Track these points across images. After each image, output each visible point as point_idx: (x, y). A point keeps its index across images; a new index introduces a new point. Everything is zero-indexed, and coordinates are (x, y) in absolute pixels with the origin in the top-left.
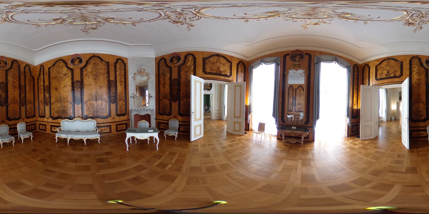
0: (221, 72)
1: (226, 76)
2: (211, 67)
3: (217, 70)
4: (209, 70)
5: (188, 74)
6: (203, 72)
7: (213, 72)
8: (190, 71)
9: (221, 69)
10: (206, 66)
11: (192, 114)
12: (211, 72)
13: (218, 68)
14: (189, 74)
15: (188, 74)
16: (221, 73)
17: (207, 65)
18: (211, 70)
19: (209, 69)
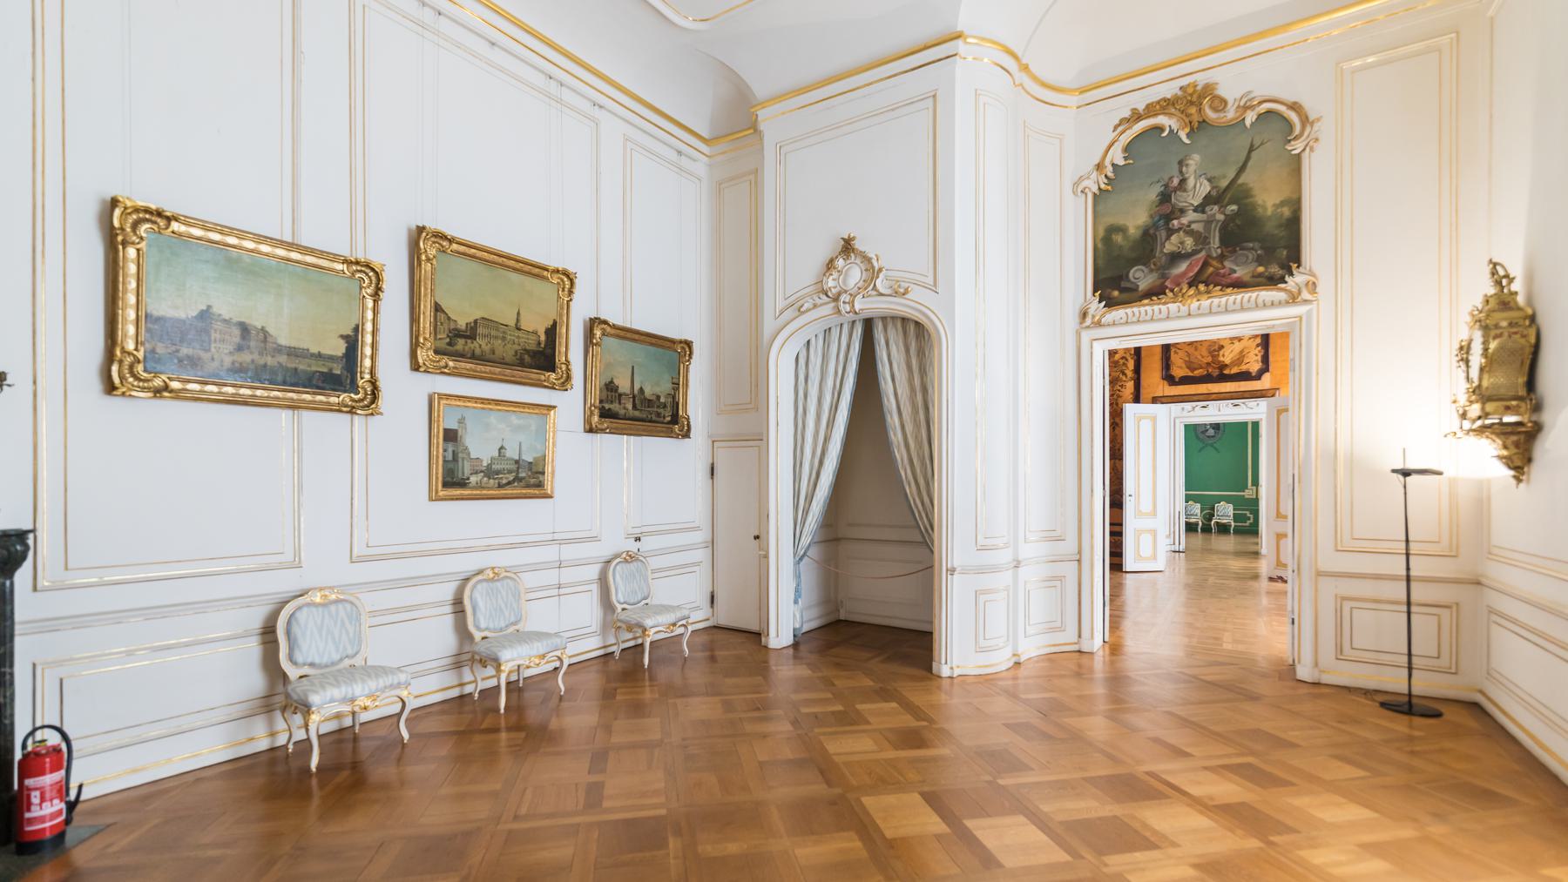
0: (1226, 365)
1: (1245, 376)
2: (1189, 355)
3: (1208, 364)
4: (1181, 367)
5: (1119, 391)
6: (1163, 379)
7: (1196, 372)
8: (1124, 378)
9: (1223, 356)
10: (1172, 353)
11: (1128, 498)
12: (1191, 374)
13: (1213, 356)
14: (1123, 390)
15: (1119, 391)
16: (1225, 372)
17: (1176, 352)
18: (1189, 368)
19: (1184, 366)
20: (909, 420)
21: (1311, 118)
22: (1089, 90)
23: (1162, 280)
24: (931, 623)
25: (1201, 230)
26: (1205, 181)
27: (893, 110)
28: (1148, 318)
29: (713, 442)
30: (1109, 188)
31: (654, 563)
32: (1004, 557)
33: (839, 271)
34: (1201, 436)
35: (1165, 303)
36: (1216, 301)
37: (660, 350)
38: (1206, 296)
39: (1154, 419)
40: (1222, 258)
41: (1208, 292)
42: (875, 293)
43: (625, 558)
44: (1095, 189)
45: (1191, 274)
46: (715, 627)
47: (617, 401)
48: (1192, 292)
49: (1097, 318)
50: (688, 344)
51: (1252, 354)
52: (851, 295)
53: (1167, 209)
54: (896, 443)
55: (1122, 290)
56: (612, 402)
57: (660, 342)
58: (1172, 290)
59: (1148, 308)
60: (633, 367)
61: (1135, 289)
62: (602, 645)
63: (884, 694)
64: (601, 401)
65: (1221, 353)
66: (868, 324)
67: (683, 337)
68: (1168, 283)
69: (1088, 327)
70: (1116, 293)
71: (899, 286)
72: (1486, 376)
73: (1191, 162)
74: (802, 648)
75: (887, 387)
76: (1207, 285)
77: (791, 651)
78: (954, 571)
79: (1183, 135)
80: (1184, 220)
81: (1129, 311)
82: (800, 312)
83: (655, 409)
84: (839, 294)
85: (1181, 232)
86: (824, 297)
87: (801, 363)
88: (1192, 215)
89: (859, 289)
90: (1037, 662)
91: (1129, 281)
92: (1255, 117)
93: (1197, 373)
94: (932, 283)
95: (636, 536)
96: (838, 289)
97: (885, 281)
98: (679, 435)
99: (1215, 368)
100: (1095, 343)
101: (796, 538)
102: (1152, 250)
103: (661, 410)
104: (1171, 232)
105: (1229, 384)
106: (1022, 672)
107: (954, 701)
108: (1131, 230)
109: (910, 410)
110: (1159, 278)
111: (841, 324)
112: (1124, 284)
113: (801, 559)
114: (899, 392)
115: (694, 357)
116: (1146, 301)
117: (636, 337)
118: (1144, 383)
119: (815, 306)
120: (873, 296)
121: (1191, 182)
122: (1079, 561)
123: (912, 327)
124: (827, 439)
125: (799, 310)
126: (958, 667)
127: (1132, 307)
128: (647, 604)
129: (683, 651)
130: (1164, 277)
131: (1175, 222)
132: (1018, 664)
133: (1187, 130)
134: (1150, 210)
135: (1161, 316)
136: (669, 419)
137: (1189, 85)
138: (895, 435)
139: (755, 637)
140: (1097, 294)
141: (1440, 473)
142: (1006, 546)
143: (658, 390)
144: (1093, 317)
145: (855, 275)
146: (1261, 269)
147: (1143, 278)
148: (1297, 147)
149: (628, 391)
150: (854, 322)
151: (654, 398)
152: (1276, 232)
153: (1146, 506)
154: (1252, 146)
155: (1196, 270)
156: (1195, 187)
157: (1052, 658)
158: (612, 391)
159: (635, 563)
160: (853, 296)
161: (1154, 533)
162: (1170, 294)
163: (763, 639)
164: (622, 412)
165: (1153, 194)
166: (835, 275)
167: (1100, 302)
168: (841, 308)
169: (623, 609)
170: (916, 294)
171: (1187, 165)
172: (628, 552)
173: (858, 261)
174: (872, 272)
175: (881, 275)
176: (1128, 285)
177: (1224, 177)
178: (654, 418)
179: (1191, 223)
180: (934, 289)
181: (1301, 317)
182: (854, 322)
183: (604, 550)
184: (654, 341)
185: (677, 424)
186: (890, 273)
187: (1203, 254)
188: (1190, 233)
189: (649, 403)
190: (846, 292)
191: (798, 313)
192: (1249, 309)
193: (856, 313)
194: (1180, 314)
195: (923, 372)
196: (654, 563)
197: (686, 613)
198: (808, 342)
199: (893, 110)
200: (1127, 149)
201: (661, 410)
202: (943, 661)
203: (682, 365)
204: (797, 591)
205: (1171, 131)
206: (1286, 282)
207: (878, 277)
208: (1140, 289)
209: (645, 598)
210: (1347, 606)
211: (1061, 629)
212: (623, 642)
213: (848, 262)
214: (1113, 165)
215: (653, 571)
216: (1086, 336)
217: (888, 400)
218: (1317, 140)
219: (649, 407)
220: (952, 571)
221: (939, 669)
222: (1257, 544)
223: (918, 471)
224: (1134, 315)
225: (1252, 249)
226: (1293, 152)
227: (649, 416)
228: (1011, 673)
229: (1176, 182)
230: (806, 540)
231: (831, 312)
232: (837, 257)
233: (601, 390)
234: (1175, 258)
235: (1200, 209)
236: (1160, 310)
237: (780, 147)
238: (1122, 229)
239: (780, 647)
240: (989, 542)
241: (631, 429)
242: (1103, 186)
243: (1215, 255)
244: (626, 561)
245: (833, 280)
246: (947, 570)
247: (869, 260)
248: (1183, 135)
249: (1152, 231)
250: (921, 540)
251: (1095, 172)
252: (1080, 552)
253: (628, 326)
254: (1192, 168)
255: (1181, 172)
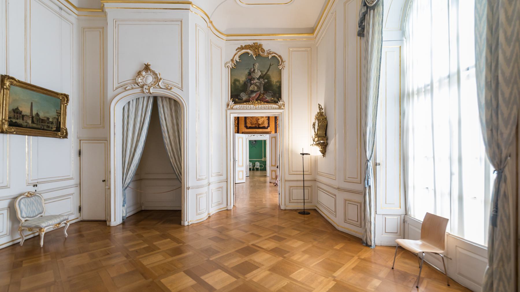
0: (260, 124)
3: (256, 123)
4: (249, 124)
13: (257, 121)
16: (260, 126)
17: (248, 119)
18: (251, 124)
20: (171, 134)
21: (283, 61)
22: (230, 36)
23: (249, 98)
24: (181, 207)
25: (259, 85)
26: (260, 71)
27: (166, 21)
28: (246, 108)
29: (80, 140)
30: (235, 67)
31: (45, 196)
32: (205, 182)
33: (143, 76)
34: (252, 143)
35: (250, 105)
36: (262, 106)
37: (49, 97)
38: (260, 104)
39: (242, 138)
40: (264, 94)
41: (261, 103)
42: (158, 87)
43: (27, 196)
44: (231, 67)
45: (256, 97)
46: (81, 221)
47: (21, 119)
48: (256, 102)
49: (232, 107)
50: (67, 96)
51: (266, 122)
52: (149, 86)
53: (250, 77)
54: (167, 143)
55: (239, 99)
56: (17, 119)
57: (49, 93)
58: (252, 101)
59: (245, 105)
60: (32, 103)
61: (242, 99)
62: (10, 240)
63: (164, 236)
64: (9, 118)
65: (259, 121)
66: (155, 99)
67: (63, 92)
68: (250, 99)
69: (229, 109)
70: (237, 100)
71: (168, 86)
72: (318, 131)
73: (256, 65)
74: (126, 224)
75: (163, 122)
76: (260, 101)
77: (121, 226)
78: (189, 188)
79: (254, 57)
80: (255, 82)
81: (240, 105)
82: (125, 90)
83: (46, 124)
84: (143, 85)
85: (254, 85)
86: (137, 85)
87: (126, 110)
88: (256, 81)
89: (152, 84)
90: (216, 215)
91: (240, 96)
92: (271, 57)
93: (253, 126)
94: (181, 87)
95: (34, 184)
96: (143, 83)
97: (162, 83)
98: (61, 137)
99: (257, 125)
100: (231, 114)
101: (124, 180)
102: (246, 89)
103: (50, 125)
104: (251, 84)
105: (261, 129)
106: (211, 219)
107: (188, 234)
108: (241, 82)
109: (172, 131)
110: (248, 97)
111: (144, 97)
112: (239, 97)
113: (126, 188)
114: (168, 125)
115: (69, 102)
116: (245, 103)
117: (34, 89)
118: (240, 128)
119: (132, 88)
120: (157, 88)
121: (256, 71)
122: (227, 182)
123: (173, 102)
124: (138, 141)
125: (125, 89)
126: (190, 221)
127: (241, 104)
128: (42, 216)
129: (64, 235)
130: (250, 97)
131: (252, 81)
132: (209, 217)
133: (255, 56)
134: (246, 77)
135: (249, 108)
136: (55, 129)
137: (256, 43)
138: (166, 140)
139: (104, 223)
140: (232, 99)
141: (309, 154)
142: (206, 178)
143: (48, 115)
144: (231, 106)
145: (150, 79)
146: (273, 99)
147: (244, 96)
148: (280, 67)
149: (29, 114)
150: (149, 97)
151: (45, 119)
152: (276, 89)
153: (241, 164)
154: (270, 64)
155: (258, 96)
156: (257, 72)
157: (219, 213)
158: (17, 113)
159: (34, 198)
160: (150, 87)
161: (243, 171)
162: (251, 102)
163: (108, 223)
164: (25, 124)
165: (247, 72)
166: (142, 78)
167: (233, 102)
168: (145, 90)
169: (26, 221)
170: (175, 90)
171: (255, 66)
172: (29, 192)
173: (151, 74)
174: (157, 79)
175: (161, 81)
176: (240, 98)
177: (264, 71)
178: (45, 128)
179: (256, 82)
180: (181, 89)
181: (281, 113)
182: (149, 97)
183: (13, 192)
184: (45, 92)
185: (60, 132)
186: (165, 81)
187: (259, 92)
188: (256, 85)
189: (43, 121)
190: (146, 85)
191: (124, 90)
192: (270, 109)
193: (151, 93)
194: (254, 108)
195: (177, 118)
196: (45, 196)
197: (66, 217)
198: (129, 102)
199: (166, 21)
200: (240, 57)
201: (50, 125)
202: (185, 220)
203: (62, 106)
204: (124, 202)
205: (251, 55)
206: (278, 103)
207: (160, 81)
208: (243, 99)
209: (40, 213)
210: (291, 188)
211: (222, 204)
212: (25, 236)
213: (147, 73)
214: (236, 61)
215: (45, 200)
216: (229, 112)
217: (164, 127)
218: (285, 67)
219: (42, 123)
220: (188, 188)
221: (184, 223)
222: (266, 173)
223: (175, 153)
224: (242, 107)
225: (271, 93)
226: (280, 69)
227: (43, 127)
228: (207, 221)
229: (252, 70)
230: (128, 181)
231: (140, 92)
232: (142, 71)
233: (9, 112)
234: (253, 92)
235: (258, 79)
236: (249, 106)
237: (116, 21)
238: (238, 81)
239: (116, 225)
240: (200, 178)
241: (30, 133)
242: (233, 66)
243: (262, 93)
244: (27, 197)
245: (141, 79)
246: (187, 188)
247: (156, 74)
248: (254, 57)
249: (246, 83)
250: (176, 178)
251: (231, 62)
252: (227, 179)
253: (29, 82)
254: (256, 67)
255: (254, 67)
